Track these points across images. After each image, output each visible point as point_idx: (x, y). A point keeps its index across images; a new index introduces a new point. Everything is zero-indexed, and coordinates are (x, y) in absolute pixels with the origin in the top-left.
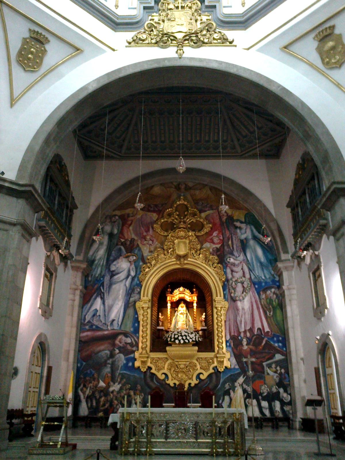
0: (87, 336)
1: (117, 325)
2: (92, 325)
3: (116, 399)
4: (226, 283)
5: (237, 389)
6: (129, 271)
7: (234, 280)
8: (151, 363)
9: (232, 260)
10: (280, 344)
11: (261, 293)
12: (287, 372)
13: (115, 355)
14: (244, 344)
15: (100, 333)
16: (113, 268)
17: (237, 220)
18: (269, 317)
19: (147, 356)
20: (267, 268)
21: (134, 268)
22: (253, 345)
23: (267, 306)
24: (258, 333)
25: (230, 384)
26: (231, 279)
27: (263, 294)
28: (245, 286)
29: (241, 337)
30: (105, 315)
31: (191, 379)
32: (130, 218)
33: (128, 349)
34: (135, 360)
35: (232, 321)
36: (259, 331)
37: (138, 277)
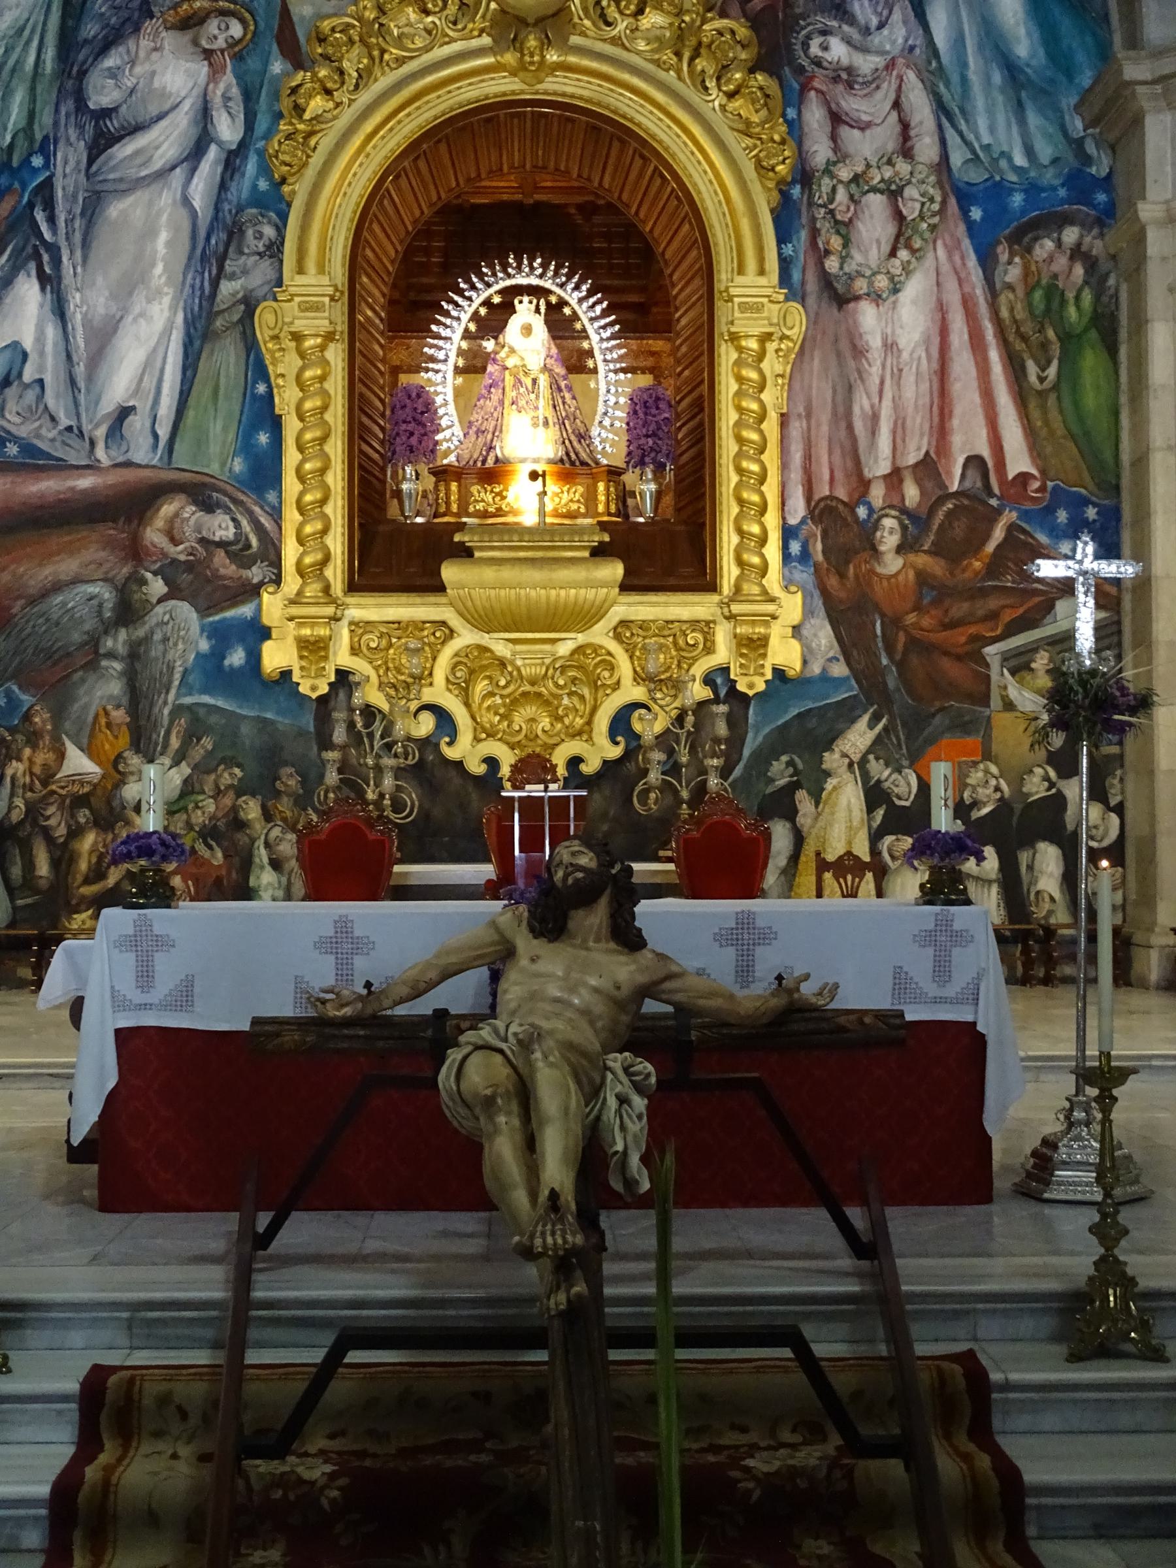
1: (146, 441)
4: (796, 191)
5: (835, 788)
6: (205, 114)
7: (845, 174)
8: (355, 651)
9: (838, 51)
13: (147, 607)
14: (882, 548)
15: (47, 486)
16: (102, 94)
18: (1041, 394)
19: (330, 610)
20: (1045, 95)
21: (235, 91)
22: (935, 552)
23: (1027, 328)
24: (968, 484)
25: (797, 759)
26: (827, 172)
27: (1010, 263)
28: (911, 211)
29: (871, 510)
30: (73, 382)
31: (585, 732)
33: (217, 576)
34: (265, 633)
35: (824, 417)
36: (973, 477)
37: (261, 153)
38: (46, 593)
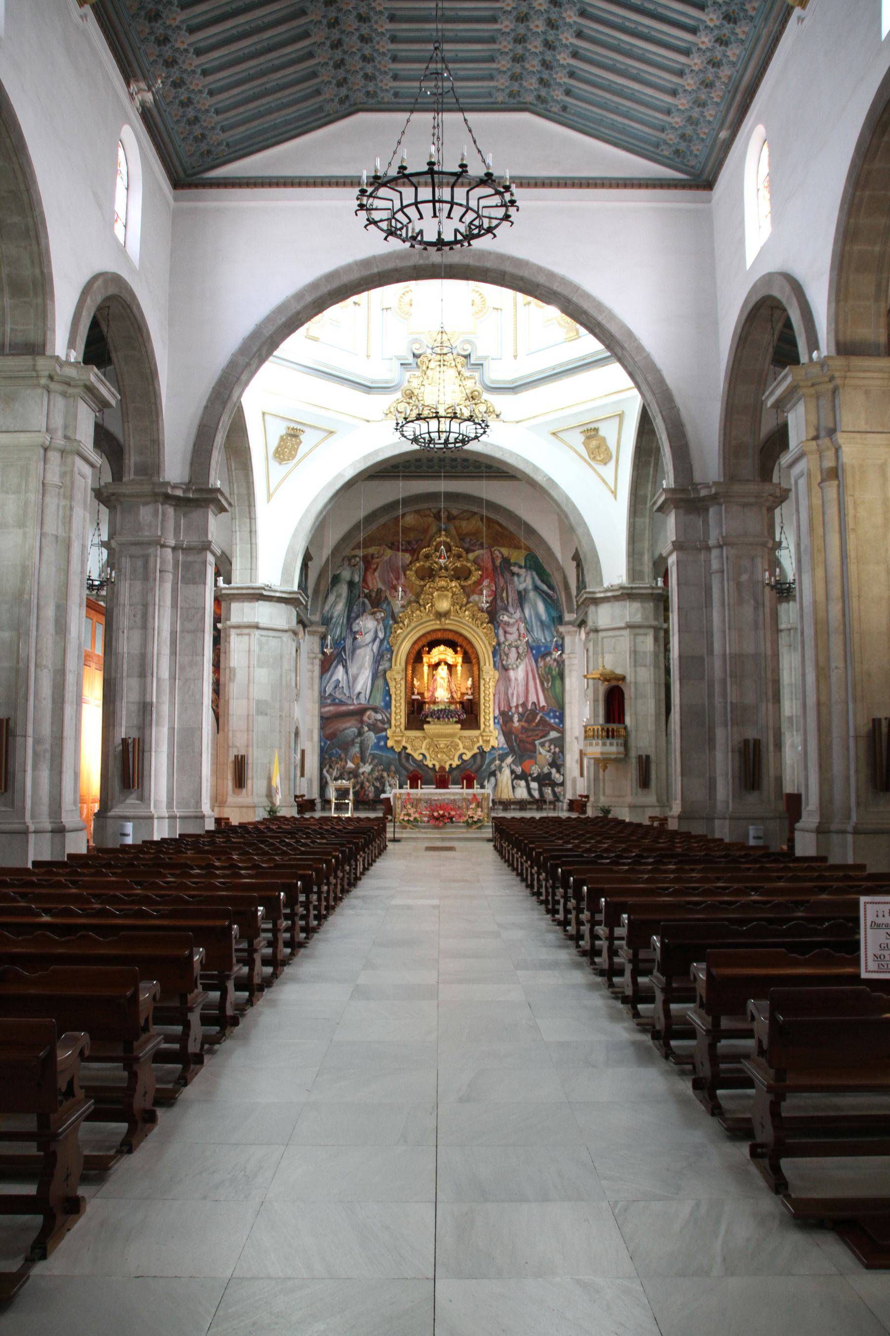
0: (329, 711)
2: (334, 699)
3: (368, 780)
6: (376, 632)
7: (507, 643)
9: (506, 618)
10: (557, 720)
11: (540, 660)
12: (562, 751)
13: (364, 733)
15: (344, 708)
16: (355, 628)
17: (515, 564)
20: (549, 628)
22: (526, 721)
28: (521, 651)
31: (453, 759)
32: (375, 561)
34: (388, 738)
38: (344, 730)
